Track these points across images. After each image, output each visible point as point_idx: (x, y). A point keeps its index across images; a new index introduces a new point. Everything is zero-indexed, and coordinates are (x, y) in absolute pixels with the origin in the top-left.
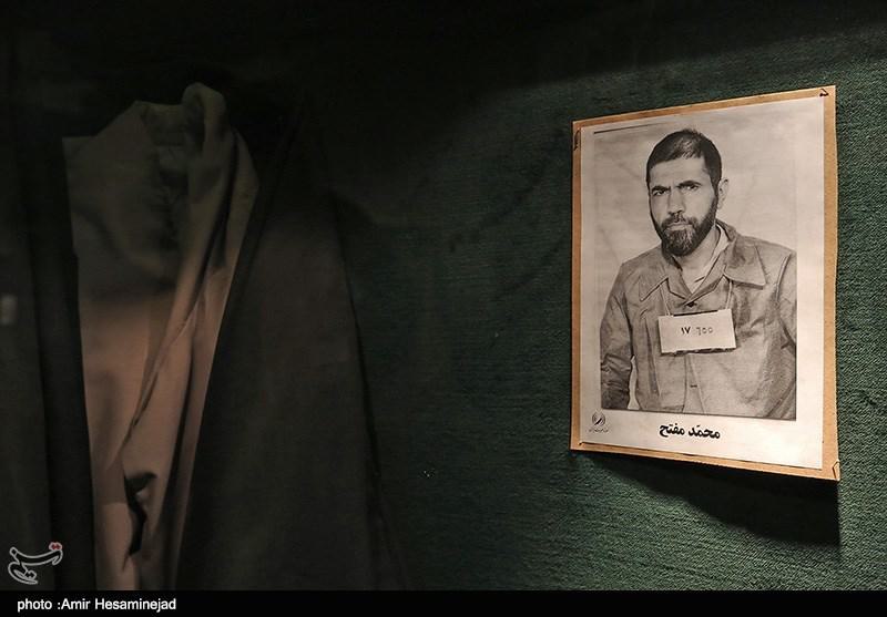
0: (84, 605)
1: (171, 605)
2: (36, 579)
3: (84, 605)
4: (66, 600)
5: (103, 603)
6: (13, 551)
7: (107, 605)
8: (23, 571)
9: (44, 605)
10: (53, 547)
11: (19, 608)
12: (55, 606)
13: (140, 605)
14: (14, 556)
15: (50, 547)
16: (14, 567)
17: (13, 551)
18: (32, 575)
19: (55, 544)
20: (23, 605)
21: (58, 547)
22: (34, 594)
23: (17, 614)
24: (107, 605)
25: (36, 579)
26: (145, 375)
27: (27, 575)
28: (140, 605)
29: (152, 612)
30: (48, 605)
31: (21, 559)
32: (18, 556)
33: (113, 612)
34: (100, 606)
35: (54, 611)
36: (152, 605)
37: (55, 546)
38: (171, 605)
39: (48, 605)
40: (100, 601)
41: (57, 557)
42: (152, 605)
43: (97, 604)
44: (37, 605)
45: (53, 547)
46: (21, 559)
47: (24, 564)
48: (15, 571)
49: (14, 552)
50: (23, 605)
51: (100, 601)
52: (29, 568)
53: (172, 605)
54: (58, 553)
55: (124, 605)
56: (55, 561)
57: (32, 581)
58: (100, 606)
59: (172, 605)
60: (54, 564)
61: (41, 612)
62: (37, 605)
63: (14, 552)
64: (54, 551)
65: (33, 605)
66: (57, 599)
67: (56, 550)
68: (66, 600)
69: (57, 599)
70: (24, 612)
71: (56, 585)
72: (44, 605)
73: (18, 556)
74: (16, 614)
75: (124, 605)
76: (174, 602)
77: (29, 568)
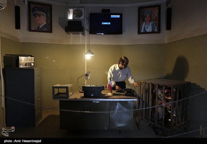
0: (20, 141)
1: (40, 141)
2: (8, 135)
3: (20, 141)
4: (15, 140)
5: (24, 141)
6: (3, 129)
7: (25, 141)
8: (5, 133)
9: (10, 141)
10: (12, 128)
11: (4, 142)
12: (13, 141)
13: (33, 141)
15: (12, 128)
16: (3, 132)
17: (3, 129)
18: (7, 134)
19: (13, 127)
20: (5, 141)
21: (14, 128)
22: (8, 139)
23: (4, 143)
24: (25, 141)
25: (8, 135)
26: (47, 58)
27: (6, 134)
28: (33, 141)
29: (36, 143)
30: (11, 141)
31: (5, 130)
32: (4, 130)
33: (26, 143)
34: (23, 142)
35: (13, 143)
36: (35, 141)
37: (13, 128)
38: (40, 141)
39: (11, 141)
40: (23, 140)
41: (13, 130)
42: (35, 141)
43: (23, 141)
44: (9, 141)
46: (5, 130)
47: (5, 132)
48: (4, 133)
50: (5, 141)
51: (23, 140)
52: (7, 133)
53: (40, 141)
54: (13, 129)
55: (29, 141)
56: (13, 131)
57: (8, 136)
58: (23, 142)
59: (40, 141)
61: (10, 143)
62: (9, 141)
63: (3, 129)
65: (8, 141)
66: (13, 140)
67: (13, 128)
68: (15, 140)
69: (13, 140)
70: (6, 143)
72: (10, 141)
73: (4, 130)
74: (4, 143)
75: (29, 141)
76: (41, 140)
77: (7, 133)
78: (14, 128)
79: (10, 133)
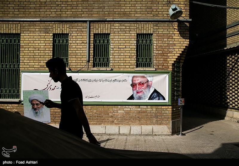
3: (22, 163)
6: (3, 148)
8: (6, 154)
9: (10, 162)
10: (14, 147)
11: (3, 163)
12: (13, 163)
14: (4, 150)
15: (13, 147)
16: (3, 153)
17: (3, 148)
18: (8, 155)
19: (15, 146)
20: (4, 163)
21: (15, 147)
22: (7, 159)
27: (7, 155)
30: (11, 162)
32: (5, 150)
33: (31, 164)
37: (15, 147)
39: (11, 162)
44: (8, 162)
45: (14, 147)
48: (4, 154)
49: (3, 148)
50: (4, 163)
52: (8, 153)
54: (15, 149)
56: (15, 151)
57: (8, 156)
60: (14, 152)
62: (8, 162)
63: (3, 148)
64: (14, 148)
67: (15, 148)
71: (13, 157)
72: (10, 162)
73: (5, 150)
77: (8, 153)
78: (15, 147)
79: (11, 154)
